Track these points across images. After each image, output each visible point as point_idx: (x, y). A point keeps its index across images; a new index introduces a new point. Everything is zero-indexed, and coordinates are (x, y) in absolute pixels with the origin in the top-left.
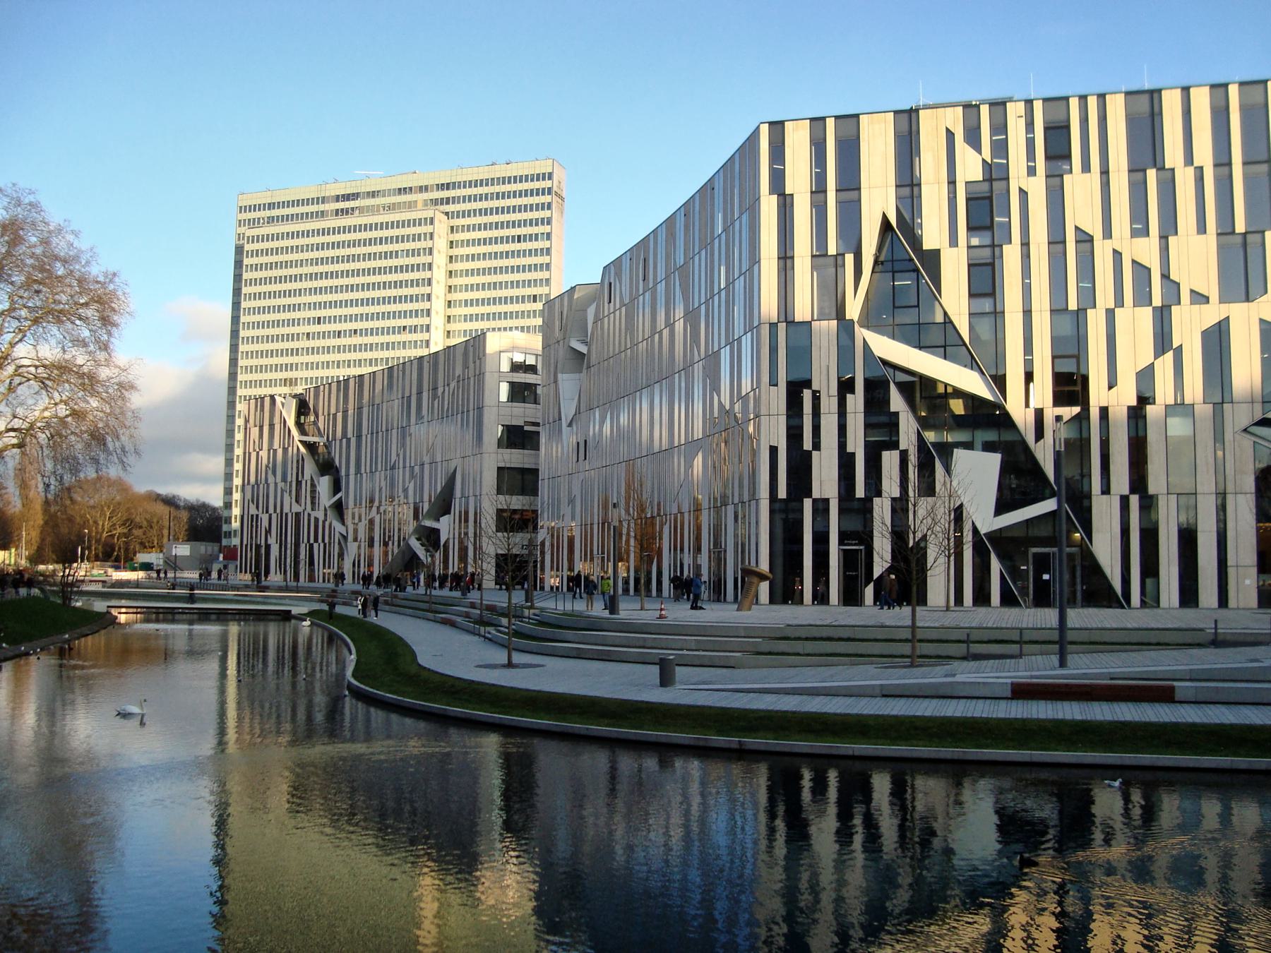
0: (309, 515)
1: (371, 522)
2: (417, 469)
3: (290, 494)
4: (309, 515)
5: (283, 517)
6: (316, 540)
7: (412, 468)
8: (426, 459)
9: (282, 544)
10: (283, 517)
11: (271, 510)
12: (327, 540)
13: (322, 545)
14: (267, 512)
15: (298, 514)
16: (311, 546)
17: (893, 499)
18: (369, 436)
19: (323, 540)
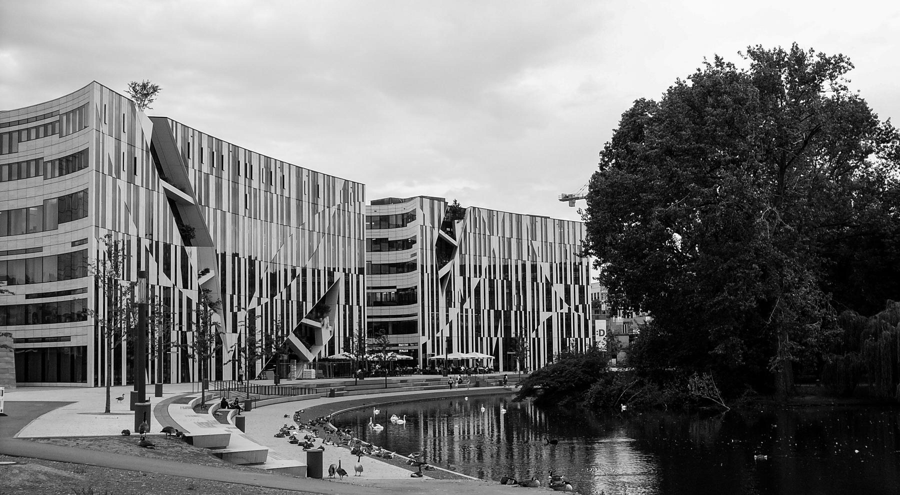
0: (180, 293)
4: (180, 293)
8: (309, 265)
17: (447, 337)
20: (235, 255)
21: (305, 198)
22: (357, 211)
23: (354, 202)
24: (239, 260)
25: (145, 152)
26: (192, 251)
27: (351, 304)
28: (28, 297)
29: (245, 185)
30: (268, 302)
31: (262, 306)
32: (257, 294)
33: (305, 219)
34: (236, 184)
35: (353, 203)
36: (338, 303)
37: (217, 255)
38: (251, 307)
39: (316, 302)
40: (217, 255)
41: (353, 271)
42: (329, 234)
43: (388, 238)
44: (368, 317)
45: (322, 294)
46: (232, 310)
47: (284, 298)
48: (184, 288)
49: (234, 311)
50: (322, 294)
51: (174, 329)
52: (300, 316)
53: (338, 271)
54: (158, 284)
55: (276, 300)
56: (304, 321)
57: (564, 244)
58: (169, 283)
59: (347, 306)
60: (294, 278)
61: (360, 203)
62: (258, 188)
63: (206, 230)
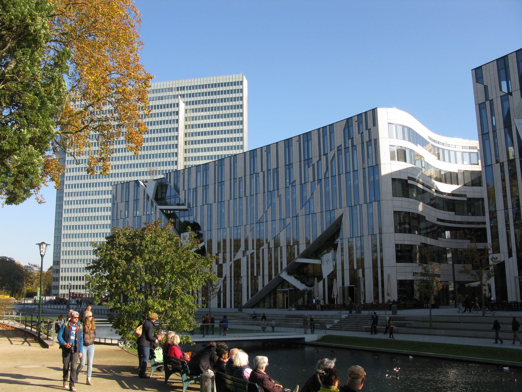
1: (237, 264)
30: (253, 253)
31: (248, 256)
32: (242, 248)
38: (236, 259)
41: (362, 201)
49: (220, 263)
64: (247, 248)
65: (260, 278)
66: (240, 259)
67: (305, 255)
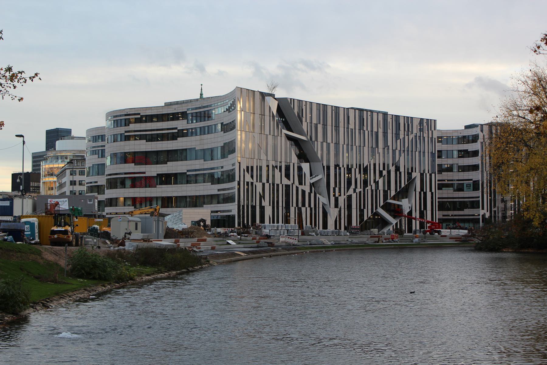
0: (297, 188)
1: (350, 197)
2: (385, 173)
3: (280, 171)
4: (297, 188)
5: (274, 188)
6: (304, 205)
7: (381, 173)
9: (274, 205)
10: (274, 188)
11: (264, 180)
12: (312, 206)
13: (308, 209)
14: (261, 181)
15: (287, 186)
16: (300, 210)
18: (345, 146)
19: (310, 205)
20: (337, 166)
21: (390, 132)
22: (430, 136)
23: (428, 131)
24: (340, 169)
25: (271, 117)
26: (306, 167)
27: (425, 191)
28: (219, 190)
29: (344, 128)
31: (357, 193)
32: (353, 186)
33: (390, 143)
34: (325, 126)
35: (427, 132)
36: (415, 190)
37: (324, 167)
38: (348, 194)
39: (398, 190)
40: (324, 167)
42: (408, 151)
43: (468, 150)
44: (439, 198)
45: (403, 185)
46: (334, 195)
47: (374, 188)
48: (299, 184)
49: (336, 196)
50: (403, 185)
51: (292, 206)
52: (385, 197)
53: (415, 172)
54: (281, 183)
55: (367, 190)
56: (389, 201)
57: (363, 130)
58: (289, 183)
59: (422, 192)
60: (381, 177)
61: (432, 131)
62: (354, 128)
63: (316, 154)
64: (356, 187)
65: (365, 210)
66: (351, 195)
67: (394, 198)
